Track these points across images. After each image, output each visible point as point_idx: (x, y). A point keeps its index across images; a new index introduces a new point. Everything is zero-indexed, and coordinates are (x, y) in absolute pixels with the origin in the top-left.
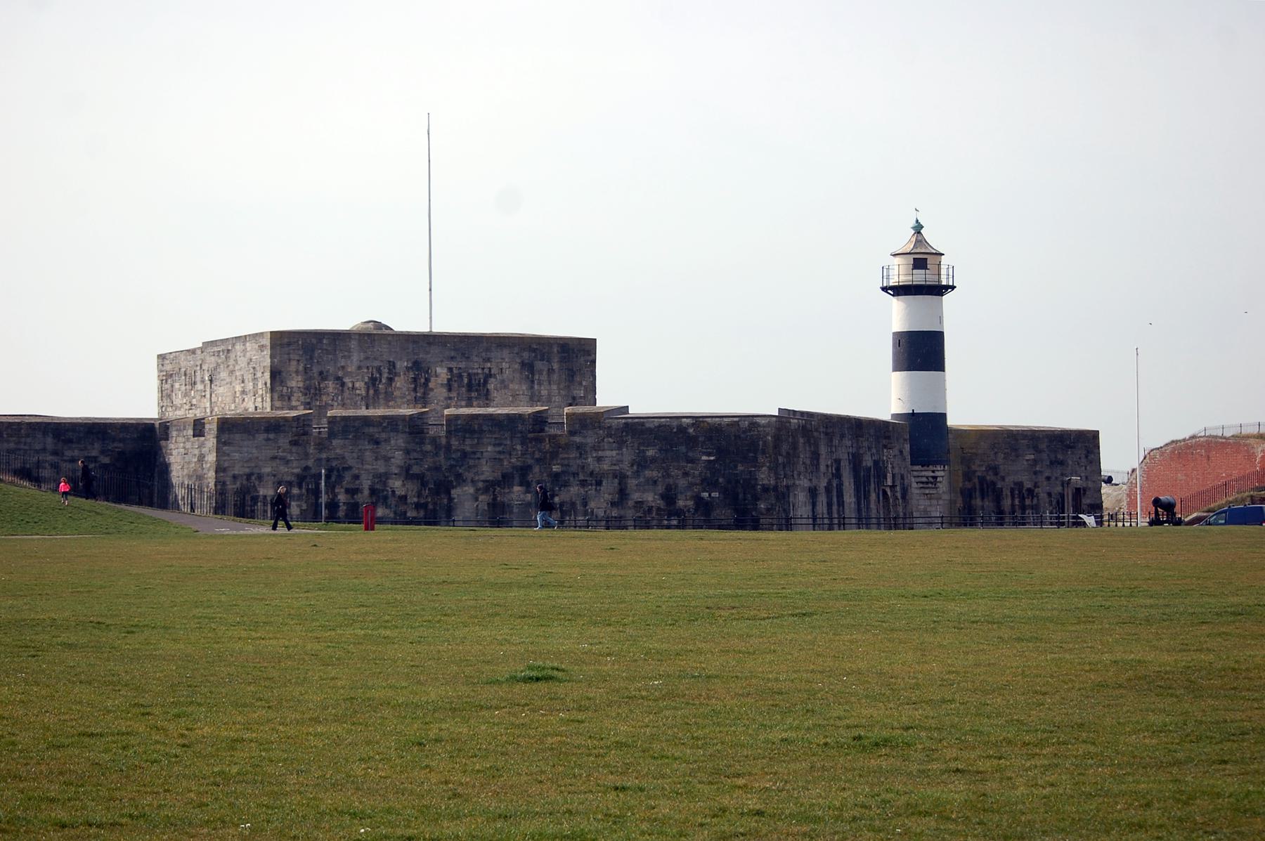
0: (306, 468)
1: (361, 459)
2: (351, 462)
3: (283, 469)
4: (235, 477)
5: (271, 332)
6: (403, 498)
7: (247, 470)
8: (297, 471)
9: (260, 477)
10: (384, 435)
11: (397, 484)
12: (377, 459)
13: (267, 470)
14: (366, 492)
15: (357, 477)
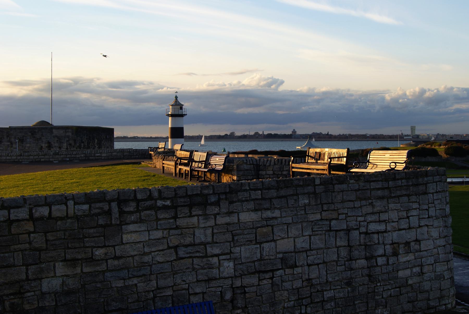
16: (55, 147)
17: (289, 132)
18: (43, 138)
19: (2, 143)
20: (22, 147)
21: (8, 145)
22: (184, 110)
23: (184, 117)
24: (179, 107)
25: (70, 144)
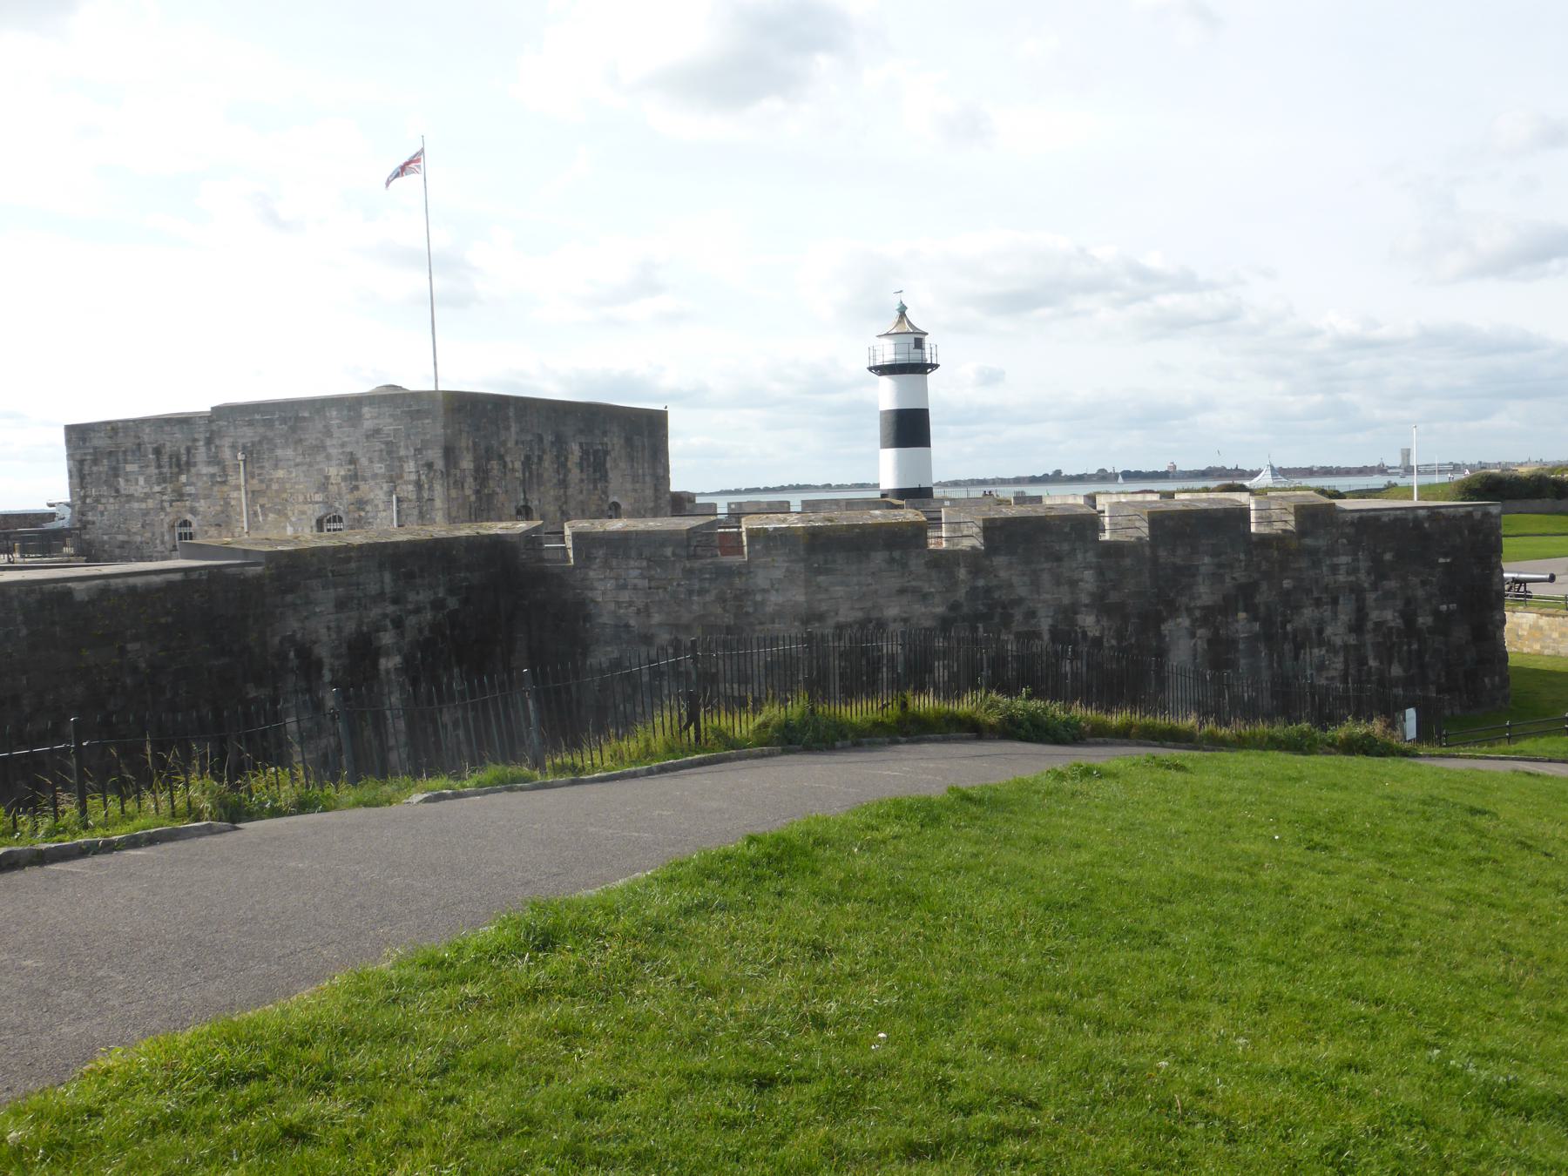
0: (954, 607)
1: (1035, 585)
2: (1022, 591)
3: (919, 609)
4: (840, 627)
5: (926, 411)
6: (1097, 642)
7: (860, 615)
8: (940, 610)
9: (881, 625)
10: (1066, 547)
11: (1088, 621)
12: (1058, 584)
13: (892, 611)
14: (1046, 636)
15: (1031, 614)
16: (375, 476)
17: (1162, 468)
18: (328, 442)
19: (193, 470)
20: (261, 481)
21: (213, 475)
22: (927, 351)
23: (932, 377)
24: (911, 339)
25: (430, 465)
